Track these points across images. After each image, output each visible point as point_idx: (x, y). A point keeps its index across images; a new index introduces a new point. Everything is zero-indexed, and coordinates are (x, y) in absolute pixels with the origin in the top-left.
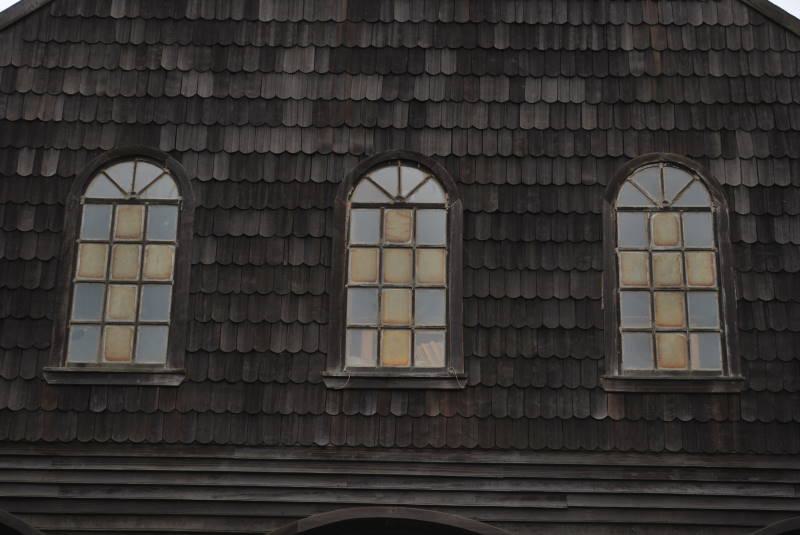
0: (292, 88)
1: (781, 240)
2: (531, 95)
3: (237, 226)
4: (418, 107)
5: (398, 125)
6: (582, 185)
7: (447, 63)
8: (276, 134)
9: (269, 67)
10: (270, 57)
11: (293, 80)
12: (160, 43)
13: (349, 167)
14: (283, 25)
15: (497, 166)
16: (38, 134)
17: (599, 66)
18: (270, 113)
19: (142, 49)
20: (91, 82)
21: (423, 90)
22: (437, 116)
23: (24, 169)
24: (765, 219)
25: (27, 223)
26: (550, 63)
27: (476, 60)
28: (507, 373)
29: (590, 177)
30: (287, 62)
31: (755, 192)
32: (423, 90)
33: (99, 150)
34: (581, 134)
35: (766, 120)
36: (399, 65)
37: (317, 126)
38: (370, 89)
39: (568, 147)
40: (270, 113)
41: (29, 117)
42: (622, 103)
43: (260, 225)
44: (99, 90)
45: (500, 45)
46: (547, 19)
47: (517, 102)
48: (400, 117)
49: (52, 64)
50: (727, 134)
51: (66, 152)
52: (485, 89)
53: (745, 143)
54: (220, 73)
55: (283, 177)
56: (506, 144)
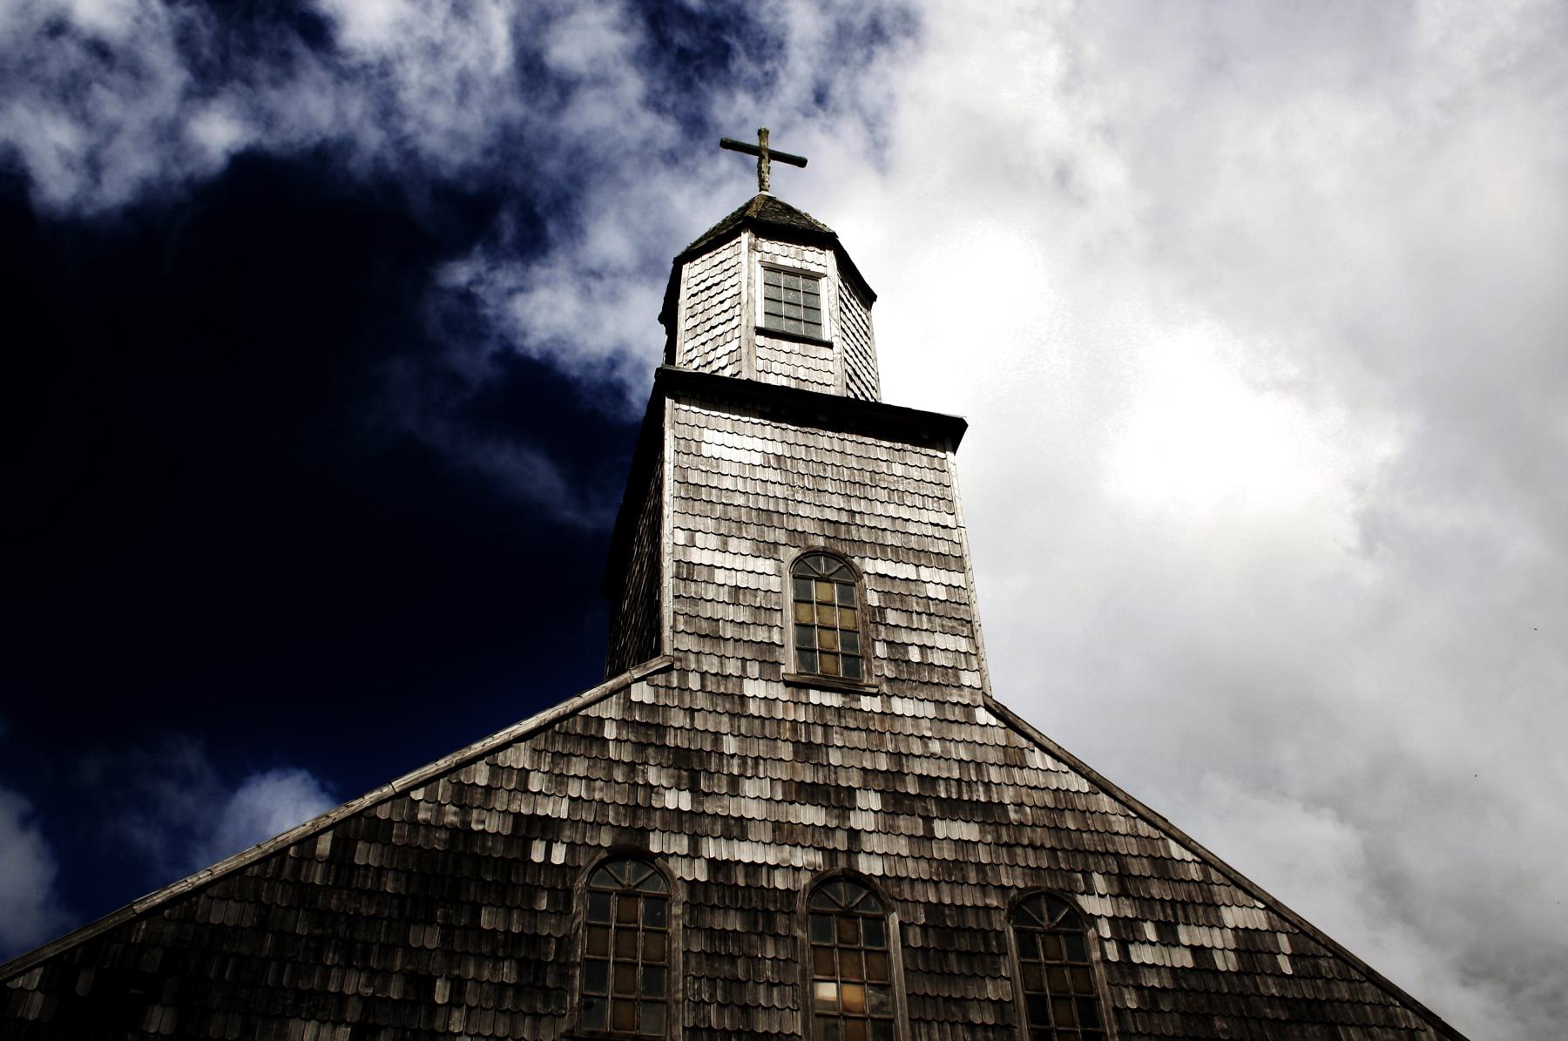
0: (753, 810)
1: (1135, 960)
2: (939, 834)
3: (718, 922)
4: (854, 834)
5: (840, 848)
6: (987, 908)
7: (875, 801)
8: (745, 846)
9: (734, 789)
10: (734, 782)
11: (752, 801)
12: (646, 763)
13: (805, 879)
14: (743, 758)
15: (919, 887)
16: (548, 828)
17: (988, 814)
18: (737, 829)
19: (632, 766)
20: (590, 789)
21: (858, 821)
23: (537, 855)
25: (543, 904)
26: (954, 809)
27: (896, 804)
30: (749, 788)
31: (1113, 920)
32: (858, 821)
33: (599, 846)
34: (980, 866)
36: (839, 800)
37: (777, 842)
38: (811, 815)
39: (973, 877)
40: (737, 829)
41: (540, 812)
43: (734, 923)
44: (597, 796)
45: (912, 791)
46: (945, 775)
47: (930, 836)
48: (840, 842)
49: (557, 771)
50: (1087, 875)
51: (572, 847)
52: (903, 823)
53: (1099, 882)
54: (695, 790)
55: (752, 882)
56: (923, 870)
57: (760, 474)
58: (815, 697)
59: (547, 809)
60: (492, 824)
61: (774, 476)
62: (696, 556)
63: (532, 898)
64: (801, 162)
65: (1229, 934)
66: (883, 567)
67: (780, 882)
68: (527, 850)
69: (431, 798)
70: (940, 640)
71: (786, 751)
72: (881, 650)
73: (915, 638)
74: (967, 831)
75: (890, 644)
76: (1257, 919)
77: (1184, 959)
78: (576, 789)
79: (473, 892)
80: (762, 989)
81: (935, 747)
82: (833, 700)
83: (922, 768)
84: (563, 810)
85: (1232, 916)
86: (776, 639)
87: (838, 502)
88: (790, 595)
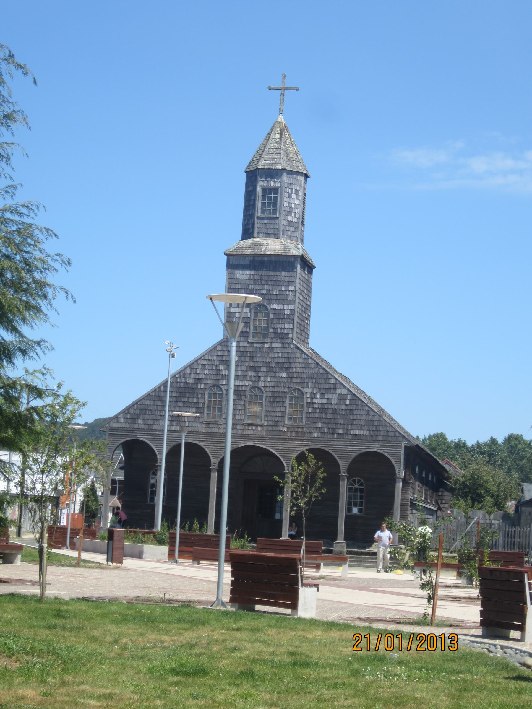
4: (259, 377)
6: (285, 392)
7: (264, 369)
13: (249, 388)
19: (216, 365)
21: (260, 374)
22: (262, 379)
24: (312, 398)
28: (270, 423)
29: (286, 390)
32: (260, 374)
35: (314, 381)
38: (251, 373)
42: (292, 377)
53: (310, 385)
56: (272, 384)
57: (248, 282)
58: (255, 345)
59: (201, 377)
60: (191, 381)
61: (252, 282)
62: (232, 310)
63: (197, 395)
64: (297, 89)
65: (337, 395)
66: (275, 306)
67: (243, 389)
68: (197, 386)
69: (180, 377)
70: (286, 326)
71: (247, 359)
72: (271, 330)
73: (280, 326)
74: (284, 375)
75: (273, 328)
76: (345, 392)
77: (325, 401)
78: (206, 372)
79: (188, 395)
80: (238, 411)
81: (280, 355)
82: (258, 345)
83: (276, 360)
84: (204, 377)
85: (339, 391)
86: (248, 331)
87: (266, 287)
88: (253, 318)
